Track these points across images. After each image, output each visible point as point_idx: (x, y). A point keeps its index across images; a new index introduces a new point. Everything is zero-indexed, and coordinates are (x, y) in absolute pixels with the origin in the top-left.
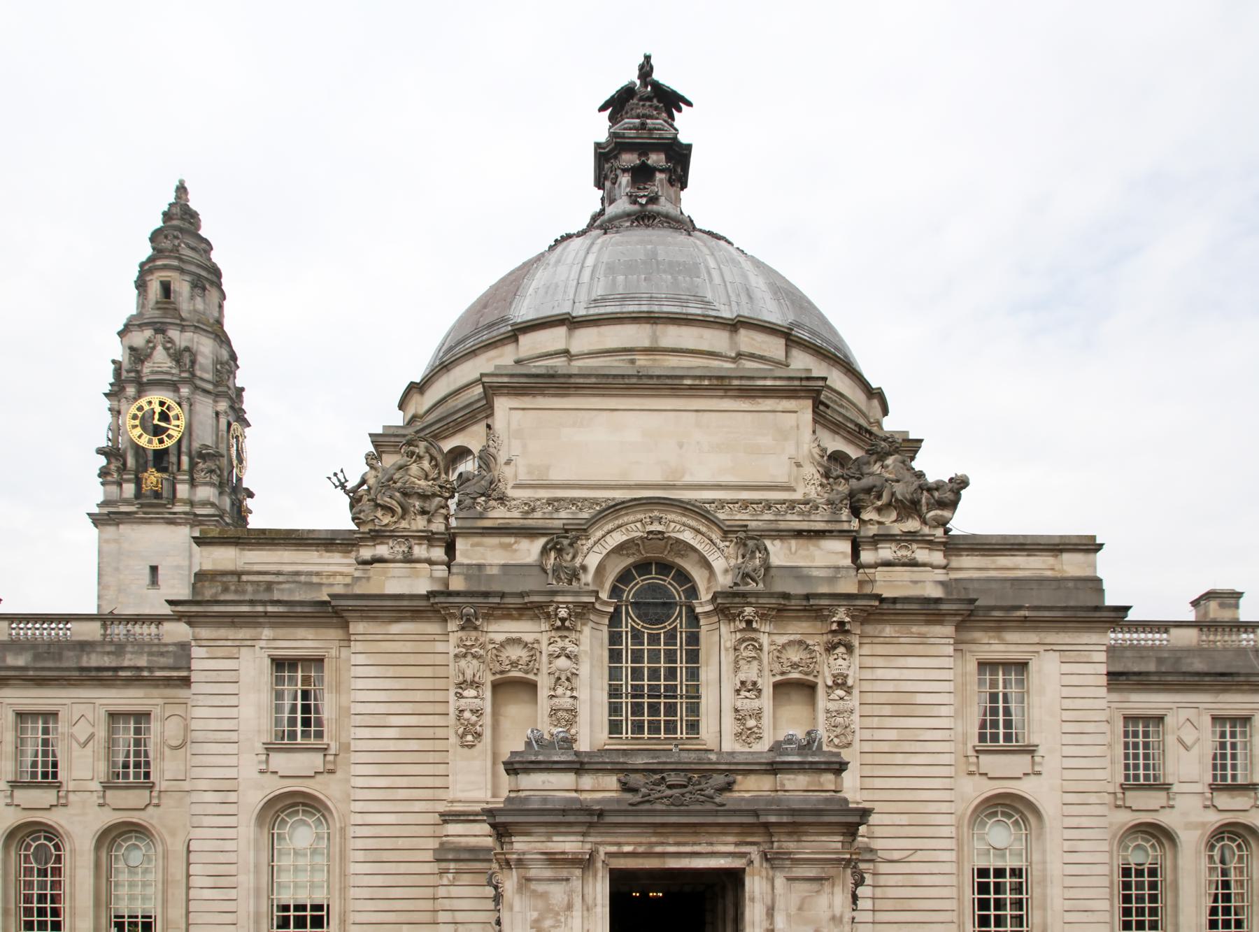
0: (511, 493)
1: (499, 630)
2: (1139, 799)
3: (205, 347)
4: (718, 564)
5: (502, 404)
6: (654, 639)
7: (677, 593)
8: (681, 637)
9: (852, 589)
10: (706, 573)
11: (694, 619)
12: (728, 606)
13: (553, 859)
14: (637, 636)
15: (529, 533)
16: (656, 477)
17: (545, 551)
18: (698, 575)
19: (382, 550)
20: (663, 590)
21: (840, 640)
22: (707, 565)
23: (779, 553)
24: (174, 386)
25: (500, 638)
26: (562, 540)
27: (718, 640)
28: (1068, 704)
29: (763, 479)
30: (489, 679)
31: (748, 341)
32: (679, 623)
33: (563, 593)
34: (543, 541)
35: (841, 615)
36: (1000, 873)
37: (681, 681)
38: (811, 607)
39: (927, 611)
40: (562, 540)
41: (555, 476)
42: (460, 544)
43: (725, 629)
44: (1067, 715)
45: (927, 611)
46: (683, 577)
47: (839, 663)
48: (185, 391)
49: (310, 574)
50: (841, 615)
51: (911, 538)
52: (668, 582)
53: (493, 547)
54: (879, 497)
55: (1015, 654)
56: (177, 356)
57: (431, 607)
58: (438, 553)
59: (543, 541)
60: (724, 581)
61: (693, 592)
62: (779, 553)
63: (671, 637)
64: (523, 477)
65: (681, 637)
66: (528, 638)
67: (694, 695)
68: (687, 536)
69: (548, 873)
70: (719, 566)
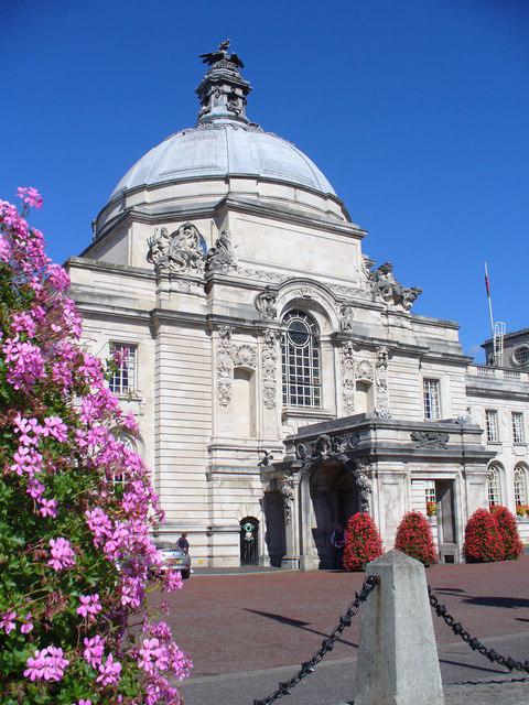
0: (239, 264)
1: (240, 339)
5: (232, 215)
6: (299, 352)
7: (309, 328)
8: (311, 352)
10: (325, 320)
11: (317, 343)
12: (336, 340)
13: (394, 474)
14: (291, 350)
16: (302, 268)
17: (258, 297)
19: (175, 285)
20: (298, 325)
21: (381, 364)
22: (325, 314)
25: (239, 344)
26: (268, 294)
27: (327, 353)
28: (455, 401)
29: (344, 276)
30: (232, 367)
32: (308, 344)
33: (272, 323)
34: (255, 293)
37: (311, 376)
41: (257, 258)
42: (216, 288)
44: (455, 407)
46: (312, 320)
49: (129, 292)
51: (400, 315)
52: (304, 320)
53: (232, 292)
54: (387, 292)
55: (435, 376)
57: (208, 323)
59: (258, 292)
60: (336, 327)
61: (316, 327)
63: (306, 351)
64: (243, 257)
65: (311, 352)
66: (252, 345)
67: (317, 384)
68: (319, 300)
69: (391, 481)
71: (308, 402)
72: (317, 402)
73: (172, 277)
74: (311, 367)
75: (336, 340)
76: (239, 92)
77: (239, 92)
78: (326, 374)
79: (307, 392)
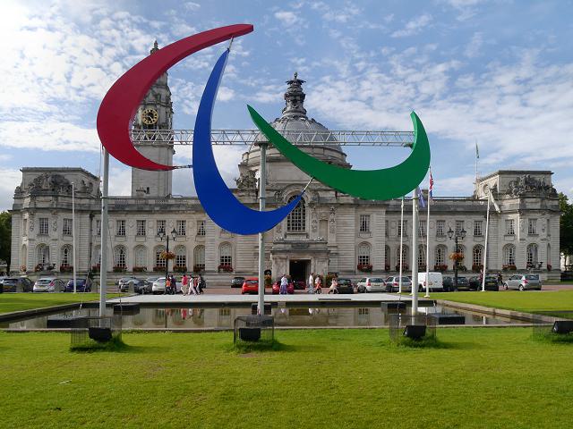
2: (477, 239)
3: (163, 93)
4: (309, 197)
9: (335, 202)
15: (273, 190)
16: (298, 179)
18: (305, 199)
23: (321, 194)
24: (155, 105)
26: (279, 192)
27: (309, 211)
31: (316, 150)
35: (333, 207)
36: (364, 257)
38: (327, 205)
39: (350, 205)
40: (279, 192)
41: (278, 179)
43: (310, 210)
45: (350, 205)
47: (332, 217)
48: (158, 106)
50: (333, 207)
55: (367, 213)
56: (156, 96)
58: (255, 194)
60: (310, 200)
62: (321, 194)
67: (304, 221)
70: (308, 197)
71: (300, 229)
72: (304, 228)
73: (242, 191)
74: (302, 216)
75: (311, 205)
76: (298, 98)
77: (298, 98)
78: (307, 218)
79: (300, 225)
